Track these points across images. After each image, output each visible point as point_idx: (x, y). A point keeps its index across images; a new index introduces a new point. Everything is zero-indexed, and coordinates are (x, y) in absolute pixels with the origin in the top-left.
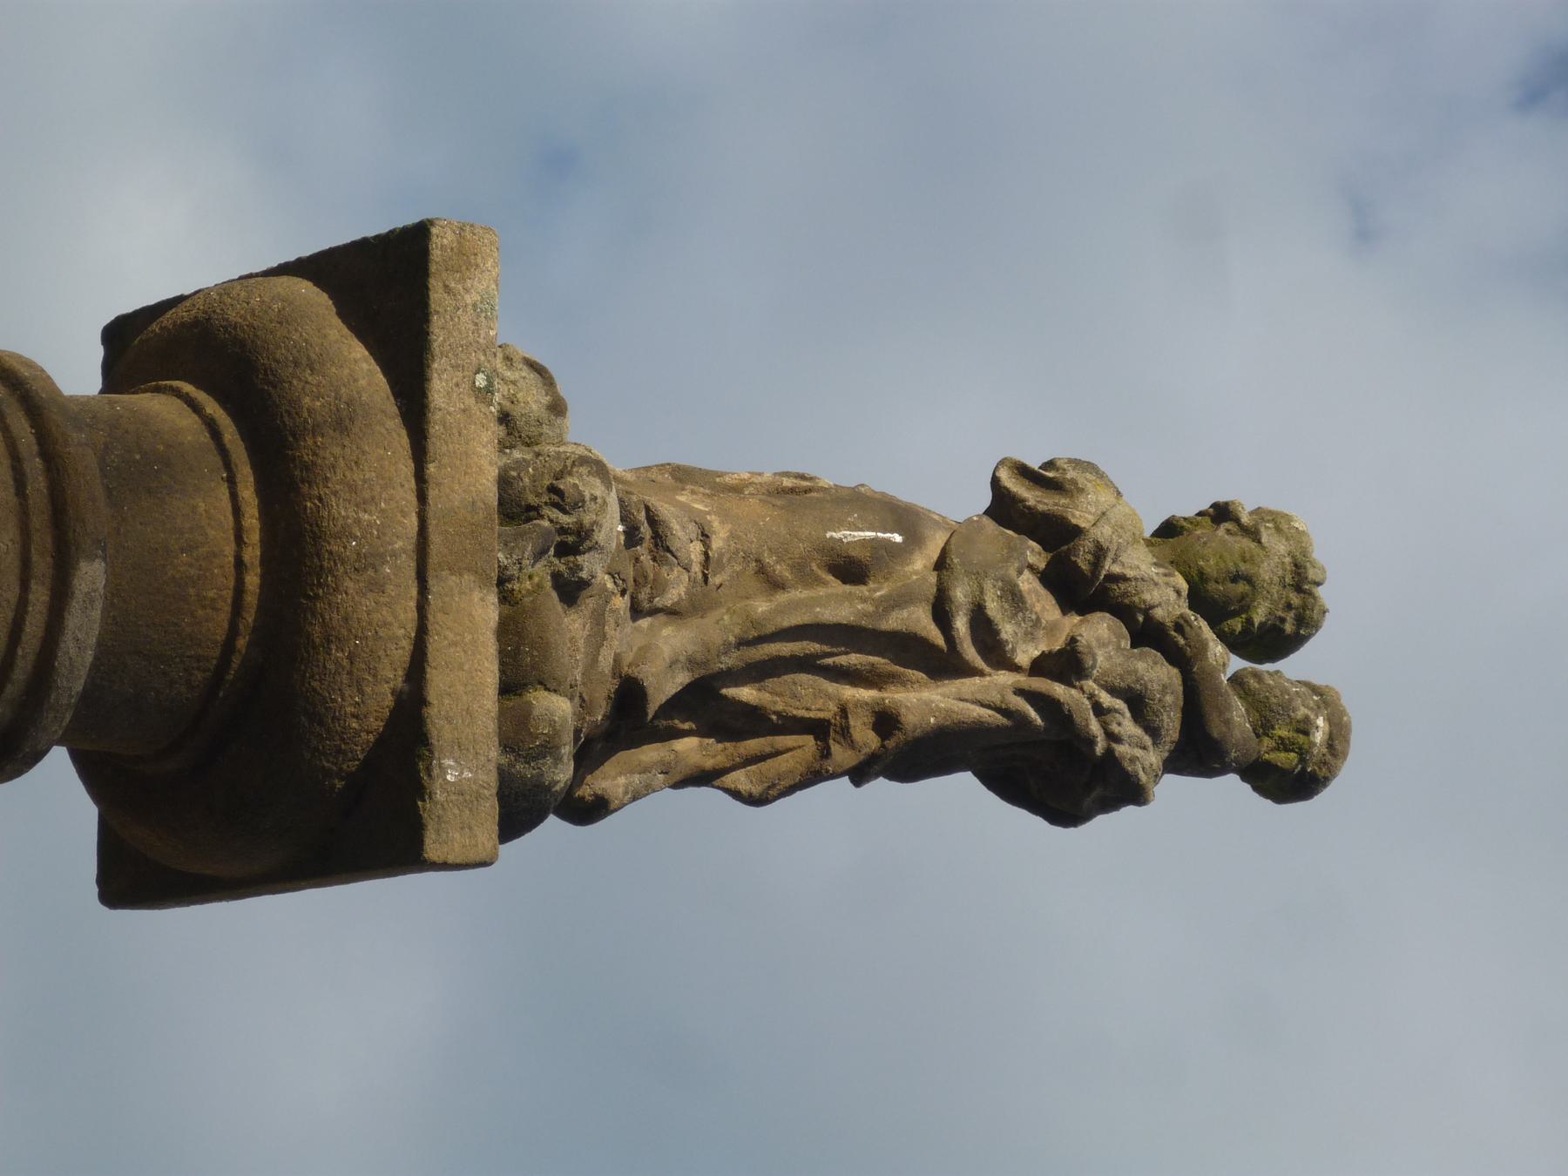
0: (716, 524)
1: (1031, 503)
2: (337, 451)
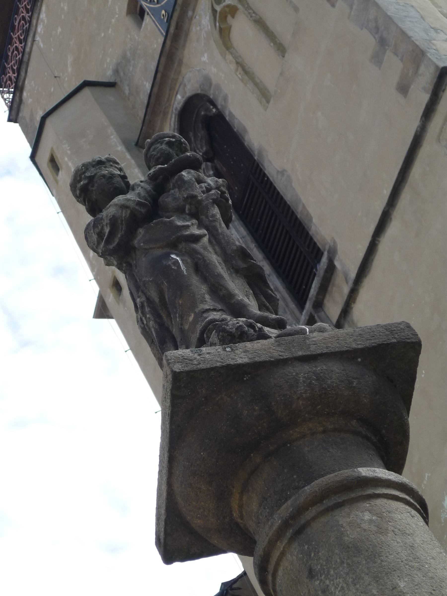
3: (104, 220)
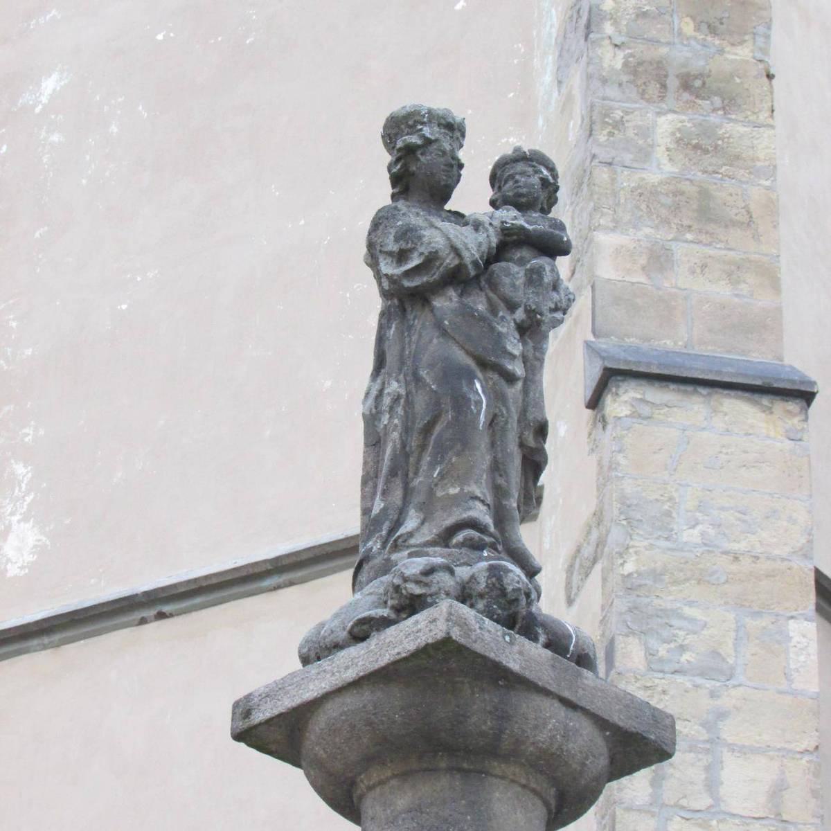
0: (470, 489)
1: (431, 280)
2: (517, 726)
3: (422, 244)
